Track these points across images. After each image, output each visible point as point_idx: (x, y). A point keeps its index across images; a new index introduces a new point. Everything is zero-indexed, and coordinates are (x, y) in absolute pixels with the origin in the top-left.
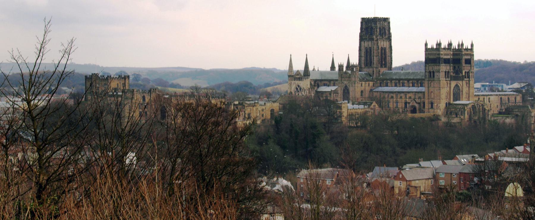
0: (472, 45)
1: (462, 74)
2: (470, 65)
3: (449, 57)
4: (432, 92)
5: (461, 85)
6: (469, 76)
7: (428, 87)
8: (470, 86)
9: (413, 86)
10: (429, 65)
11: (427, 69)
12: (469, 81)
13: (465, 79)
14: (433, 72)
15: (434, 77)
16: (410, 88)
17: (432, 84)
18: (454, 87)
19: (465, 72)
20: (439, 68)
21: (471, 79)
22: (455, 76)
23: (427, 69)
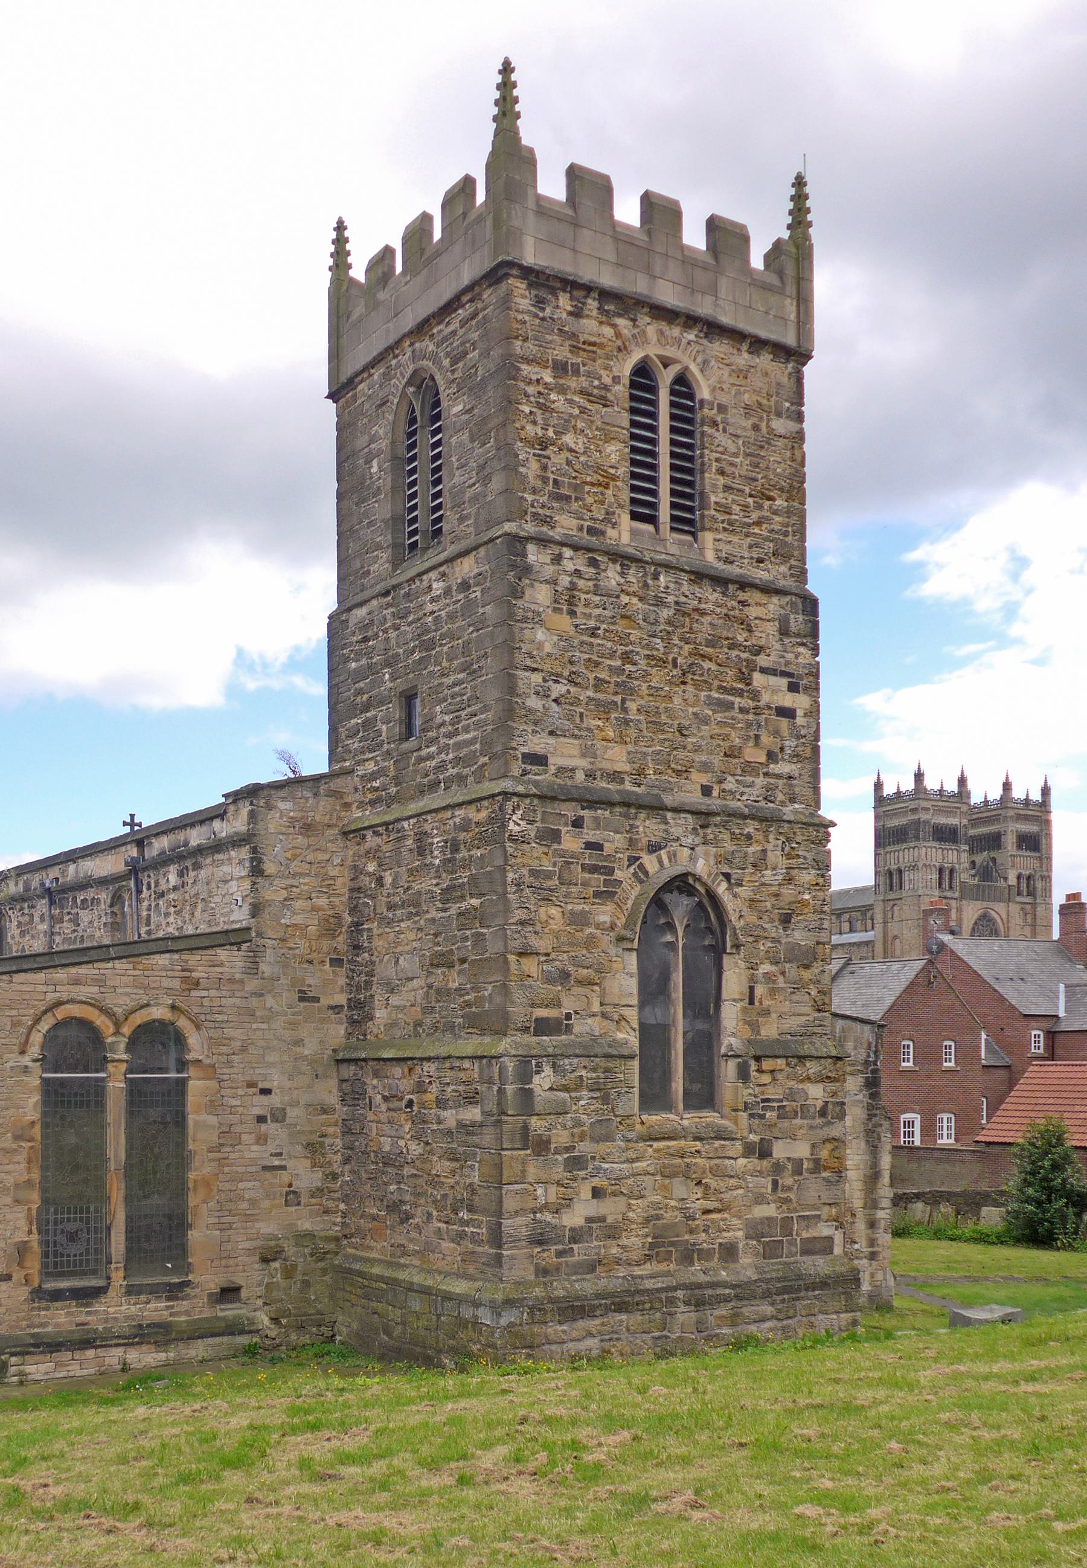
0: (1046, 791)
1: (1006, 879)
2: (1037, 855)
3: (953, 821)
4: (895, 937)
5: (1004, 916)
6: (1035, 888)
7: (885, 923)
8: (1039, 922)
9: (851, 931)
10: (888, 849)
11: (882, 863)
12: (1034, 905)
13: (1018, 899)
14: (900, 871)
15: (901, 888)
16: (844, 936)
17: (896, 913)
18: (976, 923)
19: (1019, 877)
20: (916, 855)
21: (1038, 901)
22: (978, 886)
23: (882, 863)
